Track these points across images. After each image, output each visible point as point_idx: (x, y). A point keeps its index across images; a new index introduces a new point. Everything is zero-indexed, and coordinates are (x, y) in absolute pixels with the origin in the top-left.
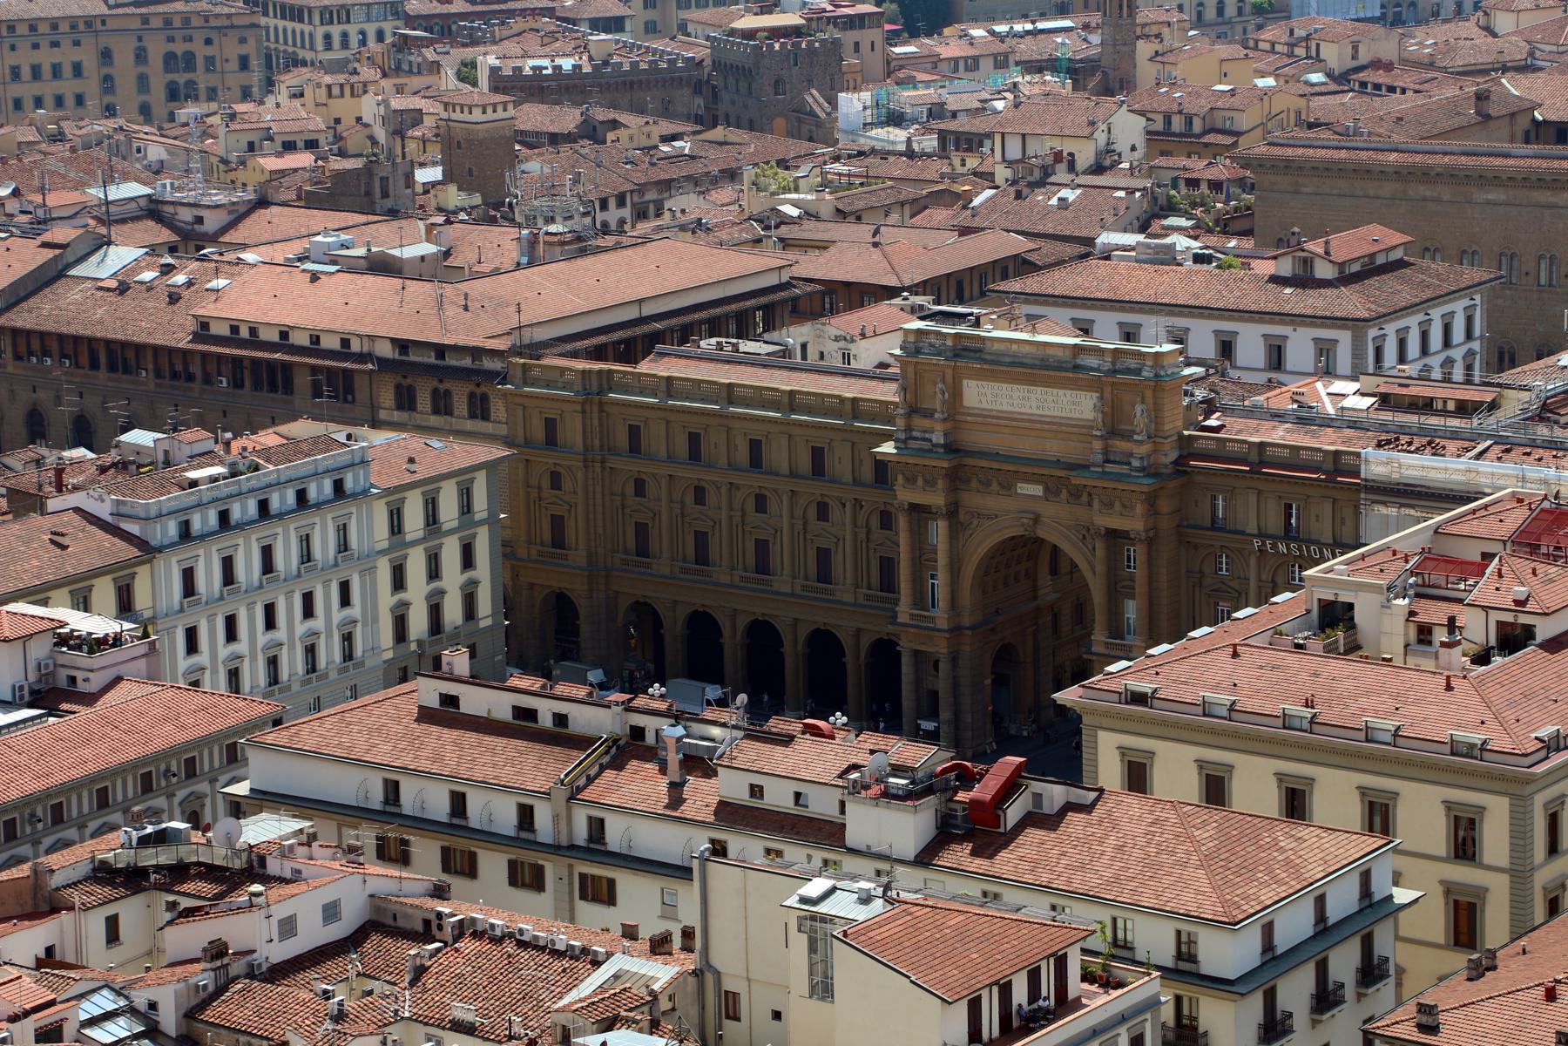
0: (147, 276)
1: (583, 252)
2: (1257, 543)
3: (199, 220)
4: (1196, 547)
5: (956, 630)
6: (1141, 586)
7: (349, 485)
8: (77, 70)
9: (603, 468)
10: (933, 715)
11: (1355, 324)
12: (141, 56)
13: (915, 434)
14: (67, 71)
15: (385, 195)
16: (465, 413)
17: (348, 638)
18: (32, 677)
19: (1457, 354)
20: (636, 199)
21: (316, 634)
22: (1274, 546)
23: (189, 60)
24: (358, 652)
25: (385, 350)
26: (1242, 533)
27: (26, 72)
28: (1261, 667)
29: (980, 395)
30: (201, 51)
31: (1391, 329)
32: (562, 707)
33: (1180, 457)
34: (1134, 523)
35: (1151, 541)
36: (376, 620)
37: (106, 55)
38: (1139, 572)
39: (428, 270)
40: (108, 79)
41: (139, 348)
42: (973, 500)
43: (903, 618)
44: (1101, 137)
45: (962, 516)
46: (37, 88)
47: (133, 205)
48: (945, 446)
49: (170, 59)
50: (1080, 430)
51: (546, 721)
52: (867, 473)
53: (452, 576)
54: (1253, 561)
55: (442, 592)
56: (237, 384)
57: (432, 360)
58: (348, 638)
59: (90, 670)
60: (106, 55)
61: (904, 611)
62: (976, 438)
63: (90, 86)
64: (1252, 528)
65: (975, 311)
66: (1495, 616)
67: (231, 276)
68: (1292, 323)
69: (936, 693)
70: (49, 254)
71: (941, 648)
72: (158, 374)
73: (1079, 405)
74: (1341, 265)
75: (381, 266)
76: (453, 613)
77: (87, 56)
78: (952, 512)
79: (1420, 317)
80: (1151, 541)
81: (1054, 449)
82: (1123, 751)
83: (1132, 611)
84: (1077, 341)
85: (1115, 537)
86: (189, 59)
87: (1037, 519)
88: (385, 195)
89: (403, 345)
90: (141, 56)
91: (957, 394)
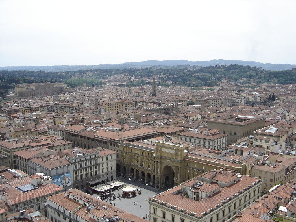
0: (92, 130)
1: (135, 129)
2: (192, 169)
5: (161, 176)
6: (179, 173)
7: (97, 156)
8: (117, 107)
11: (212, 140)
12: (123, 106)
14: (116, 107)
15: (125, 121)
18: (38, 183)
19: (224, 143)
21: (92, 172)
23: (127, 106)
25: (110, 140)
27: (113, 107)
30: (128, 105)
31: (216, 141)
32: (78, 200)
34: (178, 165)
35: (180, 168)
36: (100, 170)
37: (120, 105)
38: (179, 171)
39: (116, 131)
40: (120, 108)
43: (155, 173)
44: (196, 117)
46: (110, 109)
49: (125, 106)
51: (77, 201)
59: (44, 183)
60: (120, 105)
62: (163, 155)
63: (118, 108)
64: (191, 167)
69: (159, 182)
70: (85, 127)
71: (159, 177)
72: (91, 140)
73: (173, 152)
74: (212, 134)
75: (113, 131)
76: (110, 169)
77: (118, 106)
79: (220, 139)
80: (180, 168)
81: (171, 156)
84: (173, 144)
85: (177, 167)
86: (127, 106)
87: (169, 164)
88: (125, 121)
90: (123, 106)
91: (161, 150)
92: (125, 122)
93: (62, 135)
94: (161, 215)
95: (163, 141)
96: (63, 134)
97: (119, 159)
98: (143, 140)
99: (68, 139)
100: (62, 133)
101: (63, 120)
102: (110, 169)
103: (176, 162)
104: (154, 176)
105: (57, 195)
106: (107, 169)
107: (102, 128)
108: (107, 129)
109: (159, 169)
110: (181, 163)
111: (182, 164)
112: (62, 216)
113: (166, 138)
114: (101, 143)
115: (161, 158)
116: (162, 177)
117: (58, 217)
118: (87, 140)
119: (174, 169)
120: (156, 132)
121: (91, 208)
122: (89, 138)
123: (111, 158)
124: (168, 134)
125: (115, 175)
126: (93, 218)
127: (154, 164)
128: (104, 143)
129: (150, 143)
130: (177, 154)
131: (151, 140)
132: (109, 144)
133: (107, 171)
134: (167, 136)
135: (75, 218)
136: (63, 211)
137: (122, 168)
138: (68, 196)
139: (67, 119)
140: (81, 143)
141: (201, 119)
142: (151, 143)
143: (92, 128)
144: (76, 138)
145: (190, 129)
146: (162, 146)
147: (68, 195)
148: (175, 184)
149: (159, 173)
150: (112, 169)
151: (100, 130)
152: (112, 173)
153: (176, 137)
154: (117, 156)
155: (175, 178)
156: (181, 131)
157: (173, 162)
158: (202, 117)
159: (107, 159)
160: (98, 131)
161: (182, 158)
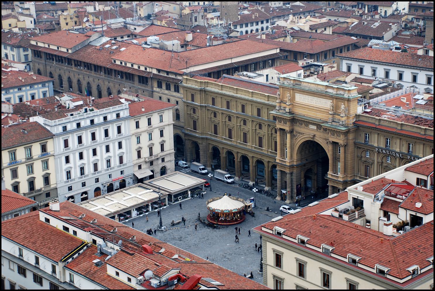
0: (107, 46)
1: (224, 43)
3: (135, 29)
4: (360, 148)
5: (292, 167)
9: (206, 109)
10: (285, 188)
13: (281, 108)
15: (196, 20)
16: (173, 90)
17: (121, 159)
20: (272, 21)
22: (382, 150)
24: (125, 161)
25: (155, 72)
26: (372, 146)
28: (321, 226)
29: (300, 98)
33: (356, 121)
34: (341, 140)
35: (345, 146)
36: (131, 152)
41: (101, 67)
42: (298, 128)
43: (277, 161)
45: (295, 133)
47: (120, 24)
48: (289, 112)
50: (326, 111)
51: (71, 232)
52: (271, 119)
53: (157, 139)
54: (376, 154)
55: (153, 144)
56: (122, 77)
57: (166, 75)
58: (121, 159)
61: (278, 158)
62: (299, 112)
65: (323, 65)
66: (409, 212)
67: (127, 47)
68: (420, 69)
69: (286, 182)
70: (85, 38)
71: (287, 171)
72: (105, 73)
75: (162, 48)
76: (157, 150)
78: (291, 132)
81: (320, 116)
82: (274, 251)
83: (340, 165)
84: (326, 83)
87: (314, 136)
88: (196, 20)
89: (159, 71)
91: (293, 99)
92: (197, 23)
93: (23, 60)
94: (295, 270)
95: (299, 75)
96: (26, 56)
97: (182, 125)
98: (245, 73)
99: (42, 69)
100: (22, 53)
101: (22, 18)
102: (157, 150)
103: (334, 132)
104: (274, 166)
105: (17, 218)
106: (151, 149)
107: (135, 41)
108: (146, 43)
109: (288, 150)
110: (346, 133)
111: (351, 136)
112: (30, 276)
113: (307, 67)
114: (133, 80)
115: (294, 120)
116: (295, 171)
117: (21, 277)
118: (93, 72)
119: (329, 150)
120: (278, 51)
121: (110, 251)
122: (97, 68)
123: (161, 121)
124: (311, 56)
125: (170, 165)
126: (116, 277)
127: (274, 136)
128: (140, 82)
129: (262, 80)
130: (335, 111)
131: (265, 72)
132: (155, 84)
133: (151, 154)
134: (311, 61)
135: (68, 280)
136: (33, 262)
137: (188, 145)
138: (47, 220)
139: (35, 16)
140: (79, 81)
141: (406, 11)
142: (267, 80)
143: (105, 39)
144: (65, 67)
145: (374, 41)
146: (297, 87)
147: (48, 217)
148: (330, 188)
149: (287, 160)
150: (162, 149)
151: (127, 45)
152: (163, 160)
153: (335, 65)
154: (177, 116)
155: (330, 172)
156: (347, 48)
157: (325, 130)
158: (410, 6)
159: (149, 123)
160: (123, 49)
161: (352, 121)
